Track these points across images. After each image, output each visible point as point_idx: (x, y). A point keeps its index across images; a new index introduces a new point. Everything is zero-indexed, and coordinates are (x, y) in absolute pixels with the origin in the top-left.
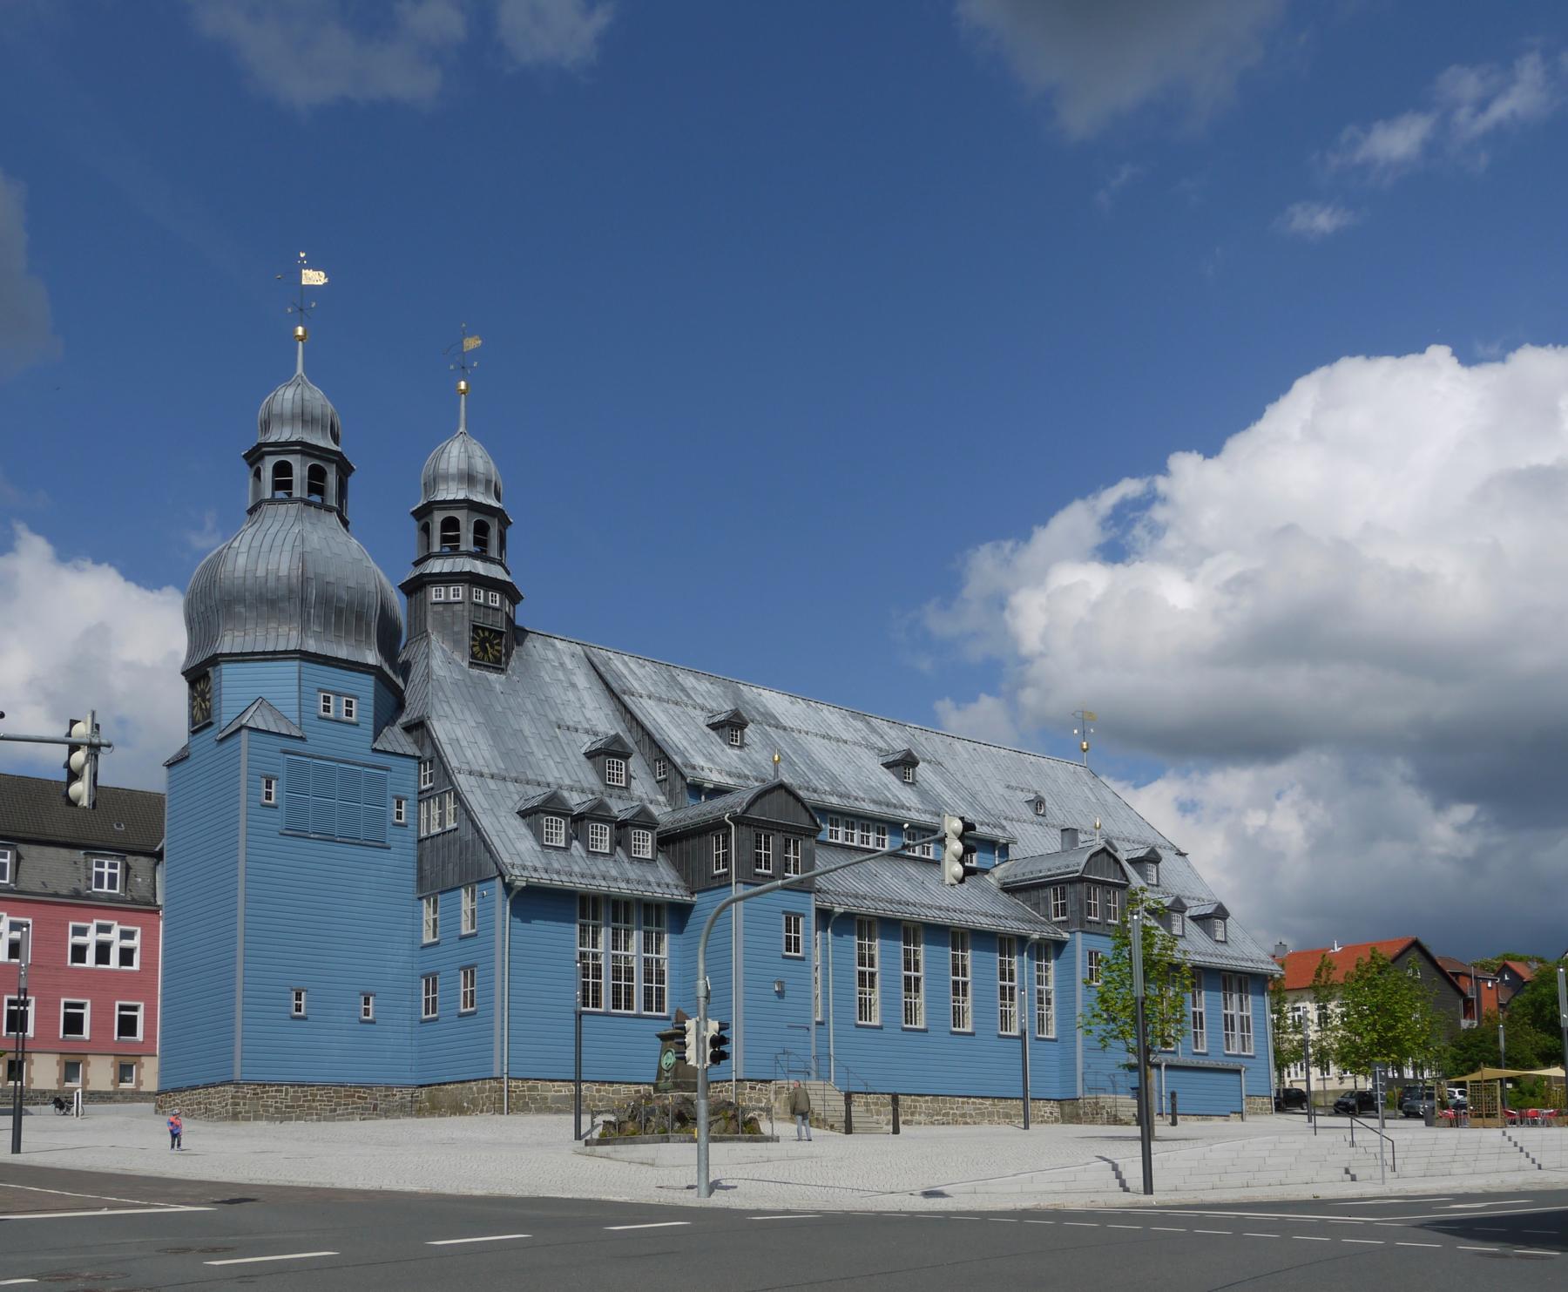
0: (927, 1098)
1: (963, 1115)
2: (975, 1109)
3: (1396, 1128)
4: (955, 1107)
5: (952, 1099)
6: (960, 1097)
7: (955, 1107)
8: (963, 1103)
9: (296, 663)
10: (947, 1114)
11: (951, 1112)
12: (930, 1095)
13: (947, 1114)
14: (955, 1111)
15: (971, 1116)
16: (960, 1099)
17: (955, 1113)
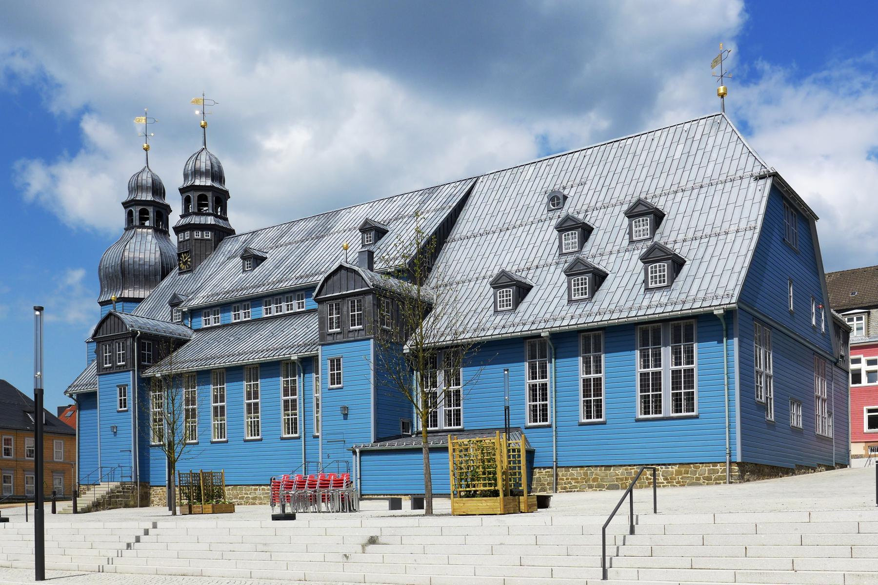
0: (229, 487)
1: (254, 498)
2: (263, 494)
3: (496, 514)
4: (249, 492)
5: (247, 488)
6: (253, 485)
7: (249, 492)
8: (256, 490)
9: (122, 303)
10: (242, 498)
11: (246, 496)
12: (231, 485)
13: (242, 498)
14: (249, 496)
15: (260, 499)
16: (253, 487)
17: (249, 497)
